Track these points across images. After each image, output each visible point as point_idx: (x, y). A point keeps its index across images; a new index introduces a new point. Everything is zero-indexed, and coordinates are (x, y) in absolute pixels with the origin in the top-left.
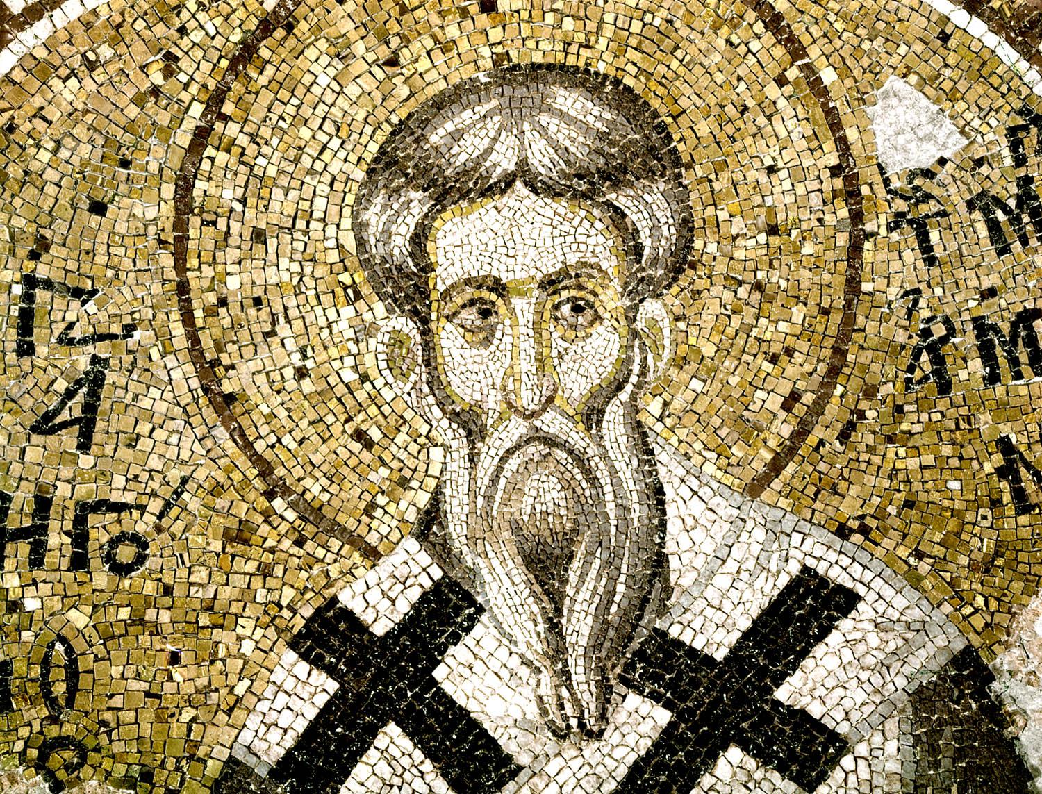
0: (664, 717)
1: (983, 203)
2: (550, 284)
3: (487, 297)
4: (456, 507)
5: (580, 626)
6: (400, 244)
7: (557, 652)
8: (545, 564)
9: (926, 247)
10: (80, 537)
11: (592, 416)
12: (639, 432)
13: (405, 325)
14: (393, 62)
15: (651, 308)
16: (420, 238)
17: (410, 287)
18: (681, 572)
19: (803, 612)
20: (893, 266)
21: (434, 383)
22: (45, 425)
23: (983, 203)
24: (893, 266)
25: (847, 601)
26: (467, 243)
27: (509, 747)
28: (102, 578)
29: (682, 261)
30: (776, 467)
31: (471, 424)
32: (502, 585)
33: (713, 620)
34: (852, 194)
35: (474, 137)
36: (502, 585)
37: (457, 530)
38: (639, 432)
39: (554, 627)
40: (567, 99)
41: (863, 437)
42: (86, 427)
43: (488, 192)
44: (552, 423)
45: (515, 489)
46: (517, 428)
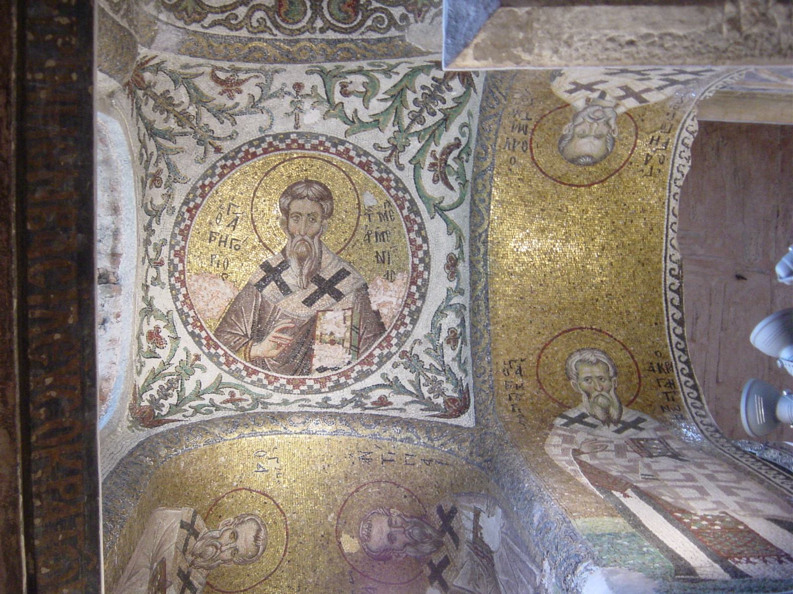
0: (317, 287)
1: (379, 213)
2: (309, 215)
3: (298, 215)
4: (288, 249)
5: (305, 271)
6: (286, 205)
7: (301, 274)
8: (301, 260)
9: (370, 219)
10: (231, 243)
11: (313, 237)
12: (320, 242)
13: (284, 218)
14: (289, 177)
15: (325, 221)
16: (289, 205)
17: (286, 211)
18: (323, 265)
19: (341, 275)
20: (364, 222)
21: (288, 228)
22: (228, 226)
23: (379, 213)
24: (364, 222)
25: (349, 273)
26: (296, 206)
27: (291, 288)
28: (234, 251)
29: (330, 214)
30: (341, 250)
31: (292, 236)
32: (294, 263)
33: (327, 275)
34: (359, 208)
35: (301, 190)
36: (294, 263)
37: (287, 253)
38: (320, 242)
39: (301, 271)
40: (316, 187)
41: (355, 247)
42: (234, 227)
43: (301, 198)
44: (306, 238)
45: (298, 248)
46: (299, 238)
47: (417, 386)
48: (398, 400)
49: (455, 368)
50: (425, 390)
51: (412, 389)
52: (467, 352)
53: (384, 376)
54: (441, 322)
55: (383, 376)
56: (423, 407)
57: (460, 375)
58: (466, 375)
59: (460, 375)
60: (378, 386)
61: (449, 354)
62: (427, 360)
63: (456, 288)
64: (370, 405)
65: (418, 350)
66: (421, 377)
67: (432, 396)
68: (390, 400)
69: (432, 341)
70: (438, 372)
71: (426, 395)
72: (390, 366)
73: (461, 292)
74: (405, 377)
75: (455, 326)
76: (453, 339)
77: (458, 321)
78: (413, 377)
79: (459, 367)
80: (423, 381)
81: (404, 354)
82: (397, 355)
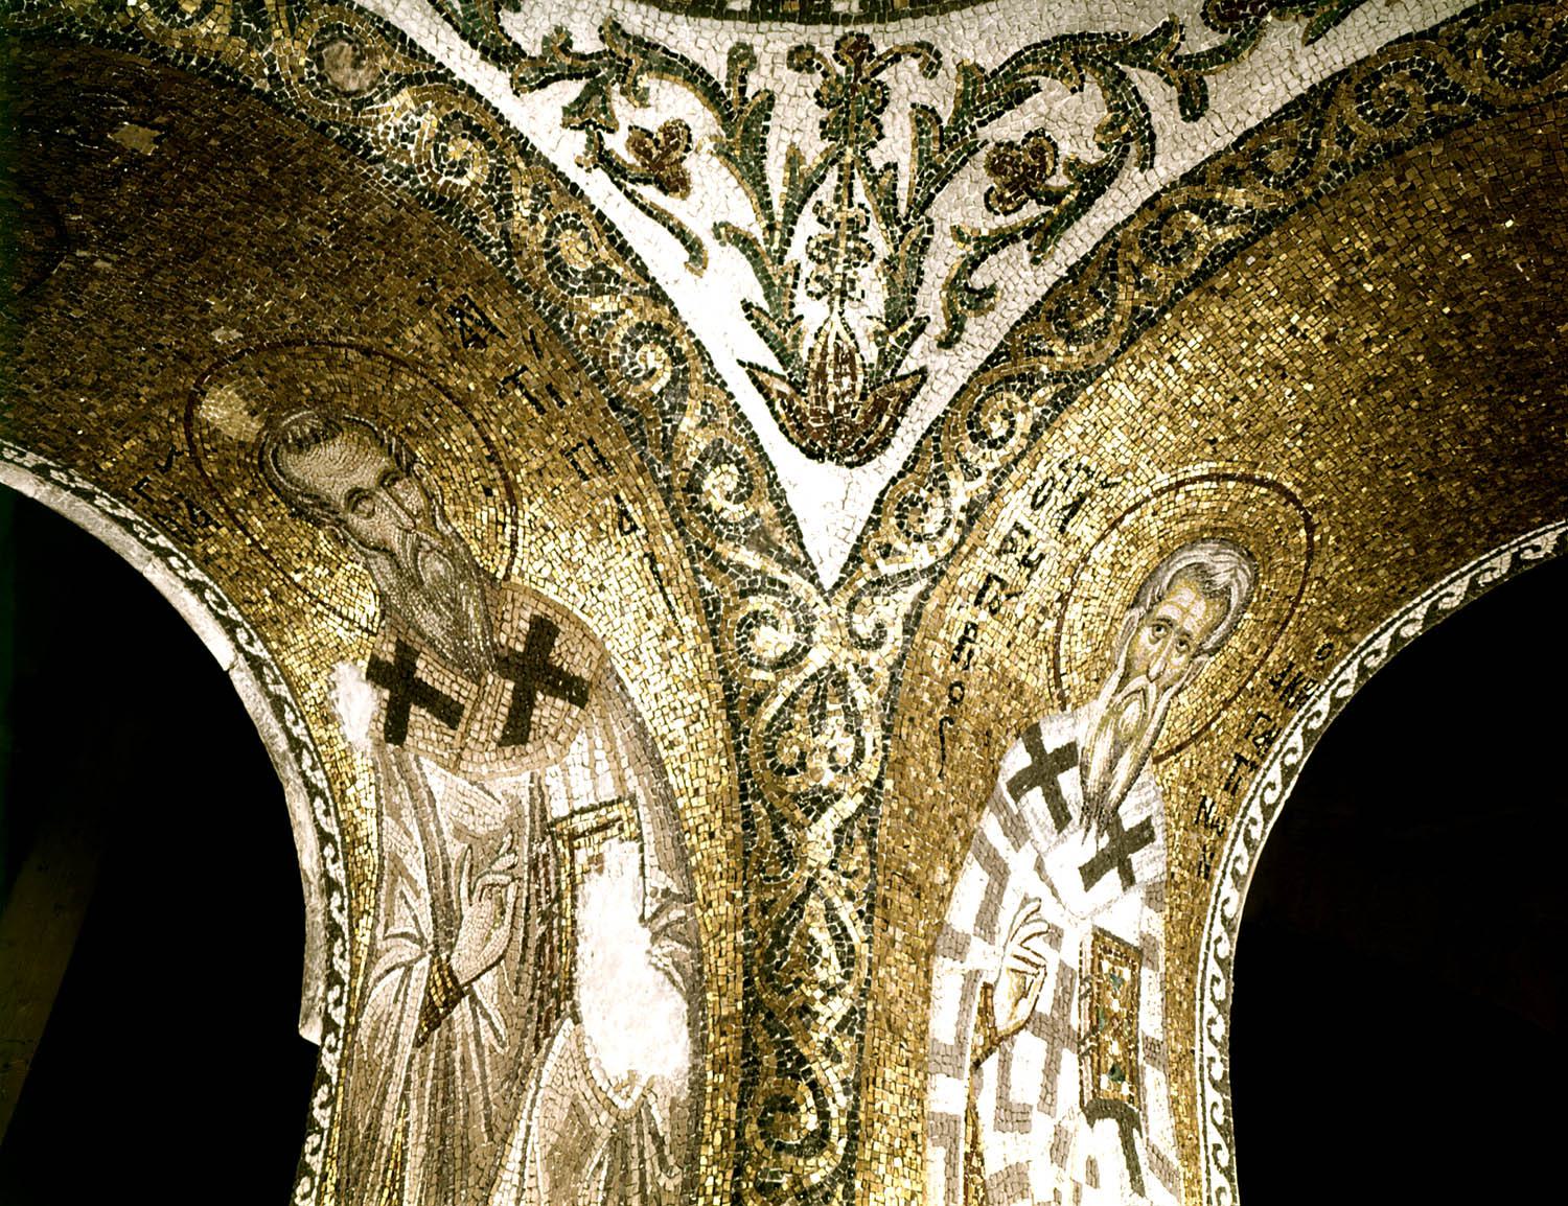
47: (803, 188)
48: (714, 194)
49: (942, 260)
50: (808, 226)
51: (777, 189)
52: (1020, 281)
53: (742, 59)
54: (1043, 81)
55: (742, 59)
56: (758, 297)
57: (931, 301)
58: (947, 343)
59: (931, 301)
60: (695, 76)
61: (964, 204)
62: (896, 145)
63: (1195, 61)
64: (617, 143)
65: (906, 83)
66: (833, 175)
67: (808, 268)
68: (691, 164)
69: (966, 104)
70: (890, 218)
71: (797, 252)
72: (783, 48)
73: (1193, 104)
74: (797, 125)
75: (1066, 149)
76: (1020, 171)
77: (1091, 155)
78: (814, 149)
79: (952, 285)
80: (825, 192)
81: (860, 48)
82: (839, 31)
